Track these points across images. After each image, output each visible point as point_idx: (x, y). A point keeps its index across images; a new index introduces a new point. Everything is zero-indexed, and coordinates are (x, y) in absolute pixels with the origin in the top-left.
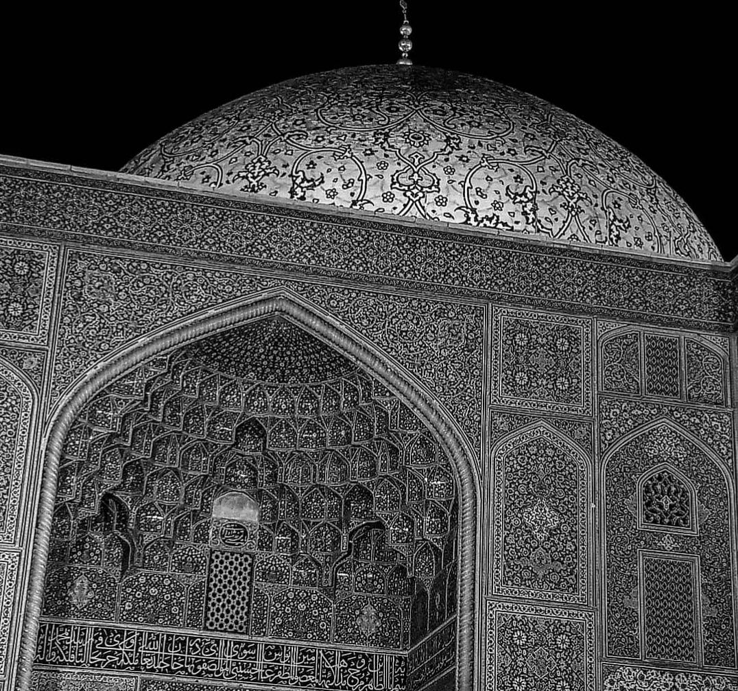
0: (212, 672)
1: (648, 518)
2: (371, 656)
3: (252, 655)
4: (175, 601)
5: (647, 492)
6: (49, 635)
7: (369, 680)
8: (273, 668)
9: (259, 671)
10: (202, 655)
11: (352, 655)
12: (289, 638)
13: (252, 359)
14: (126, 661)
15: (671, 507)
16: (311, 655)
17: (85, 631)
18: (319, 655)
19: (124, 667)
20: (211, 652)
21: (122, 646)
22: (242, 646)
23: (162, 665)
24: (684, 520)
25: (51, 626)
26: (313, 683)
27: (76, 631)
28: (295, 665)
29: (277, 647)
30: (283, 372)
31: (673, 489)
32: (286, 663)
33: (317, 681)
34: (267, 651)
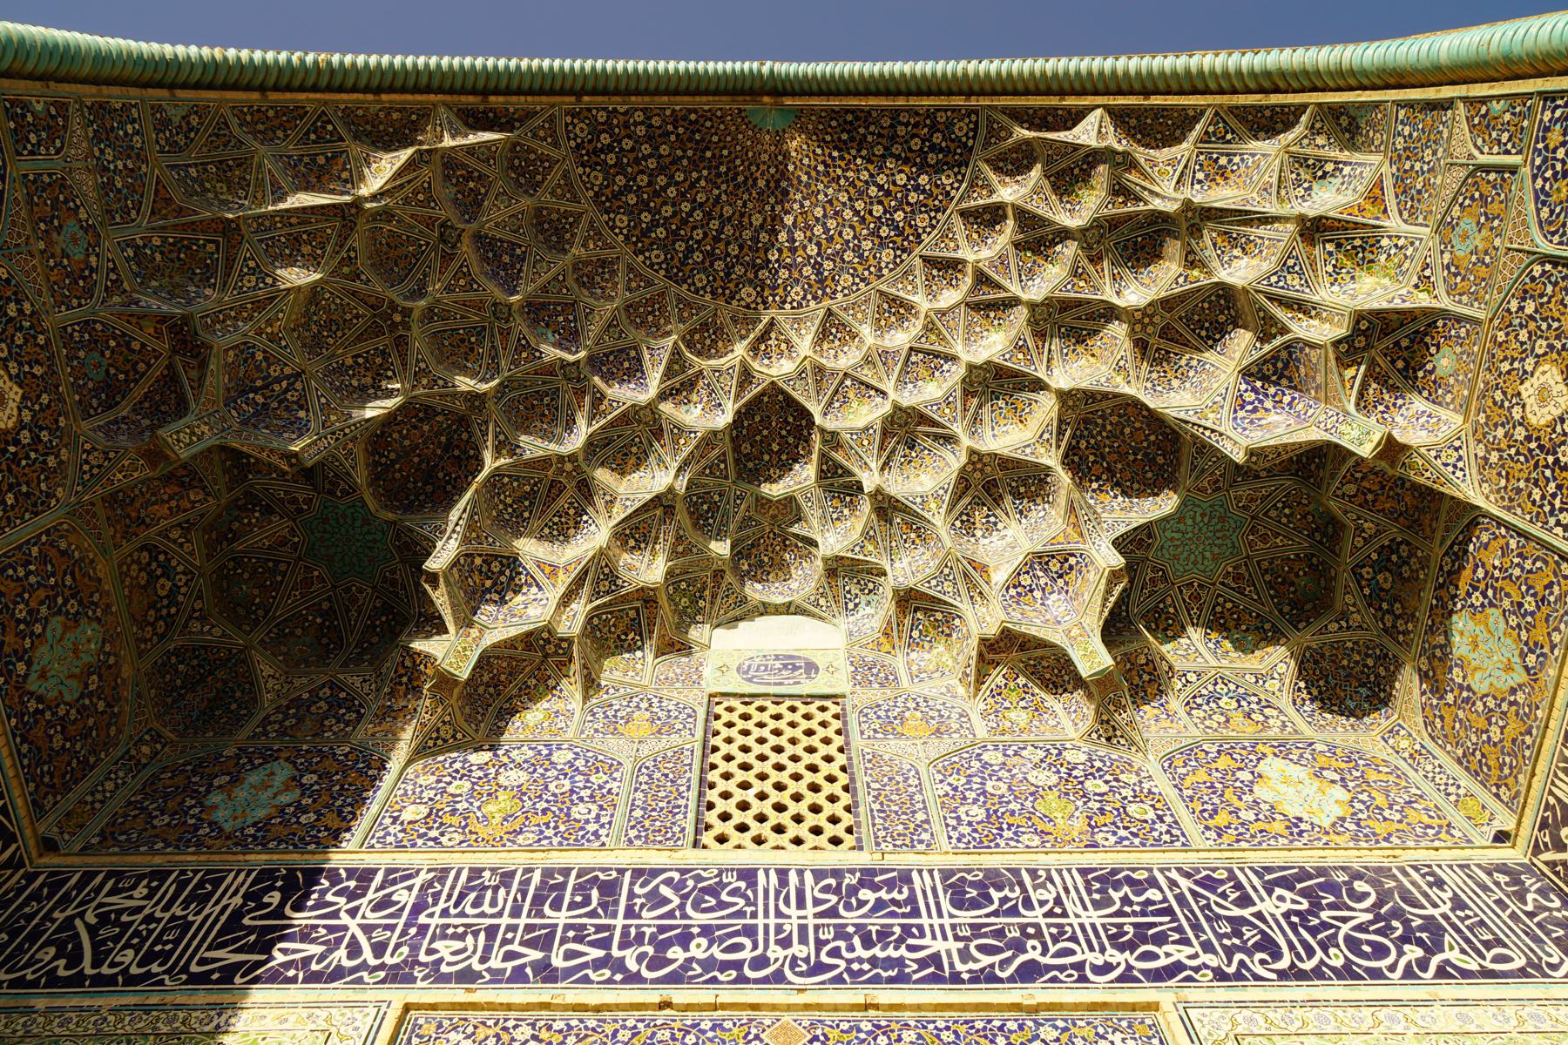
0: (738, 965)
3: (894, 902)
4: (584, 793)
6: (66, 900)
9: (939, 946)
10: (685, 916)
13: (741, 247)
14: (354, 950)
17: (217, 883)
18: (1173, 884)
19: (338, 974)
20: (722, 905)
21: (353, 913)
22: (850, 880)
23: (510, 956)
25: (88, 877)
26: (1197, 969)
27: (182, 885)
28: (1094, 917)
30: (818, 267)
32: (1047, 915)
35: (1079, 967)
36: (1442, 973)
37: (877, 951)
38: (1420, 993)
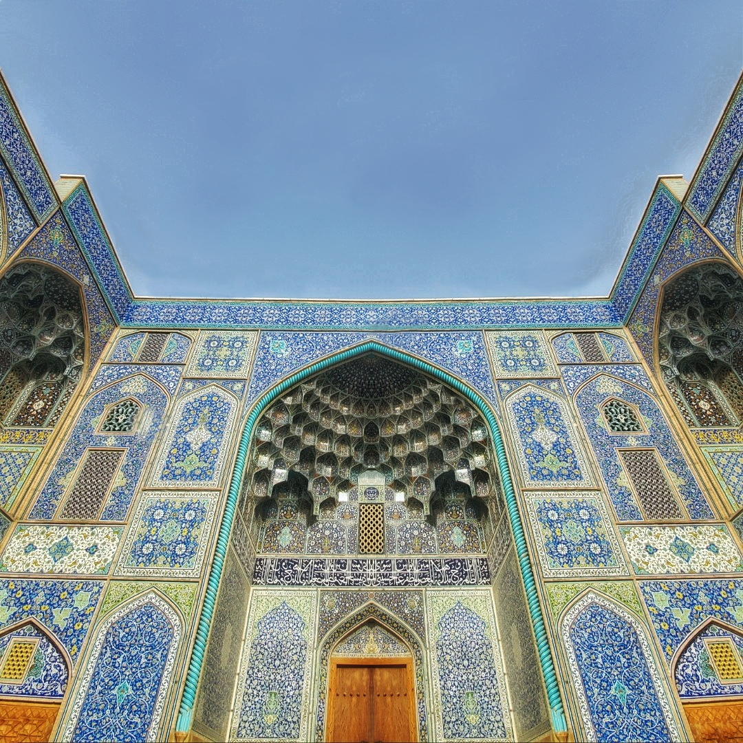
1: (613, 428)
2: (464, 560)
5: (607, 413)
7: (465, 577)
8: (403, 575)
9: (394, 578)
11: (452, 561)
12: (410, 554)
15: (626, 420)
16: (426, 564)
22: (382, 562)
24: (637, 426)
28: (416, 571)
29: (404, 560)
31: (623, 410)
33: (432, 581)
34: (398, 564)
35: (413, 582)
36: (463, 584)
37: (385, 580)
38: (458, 588)
